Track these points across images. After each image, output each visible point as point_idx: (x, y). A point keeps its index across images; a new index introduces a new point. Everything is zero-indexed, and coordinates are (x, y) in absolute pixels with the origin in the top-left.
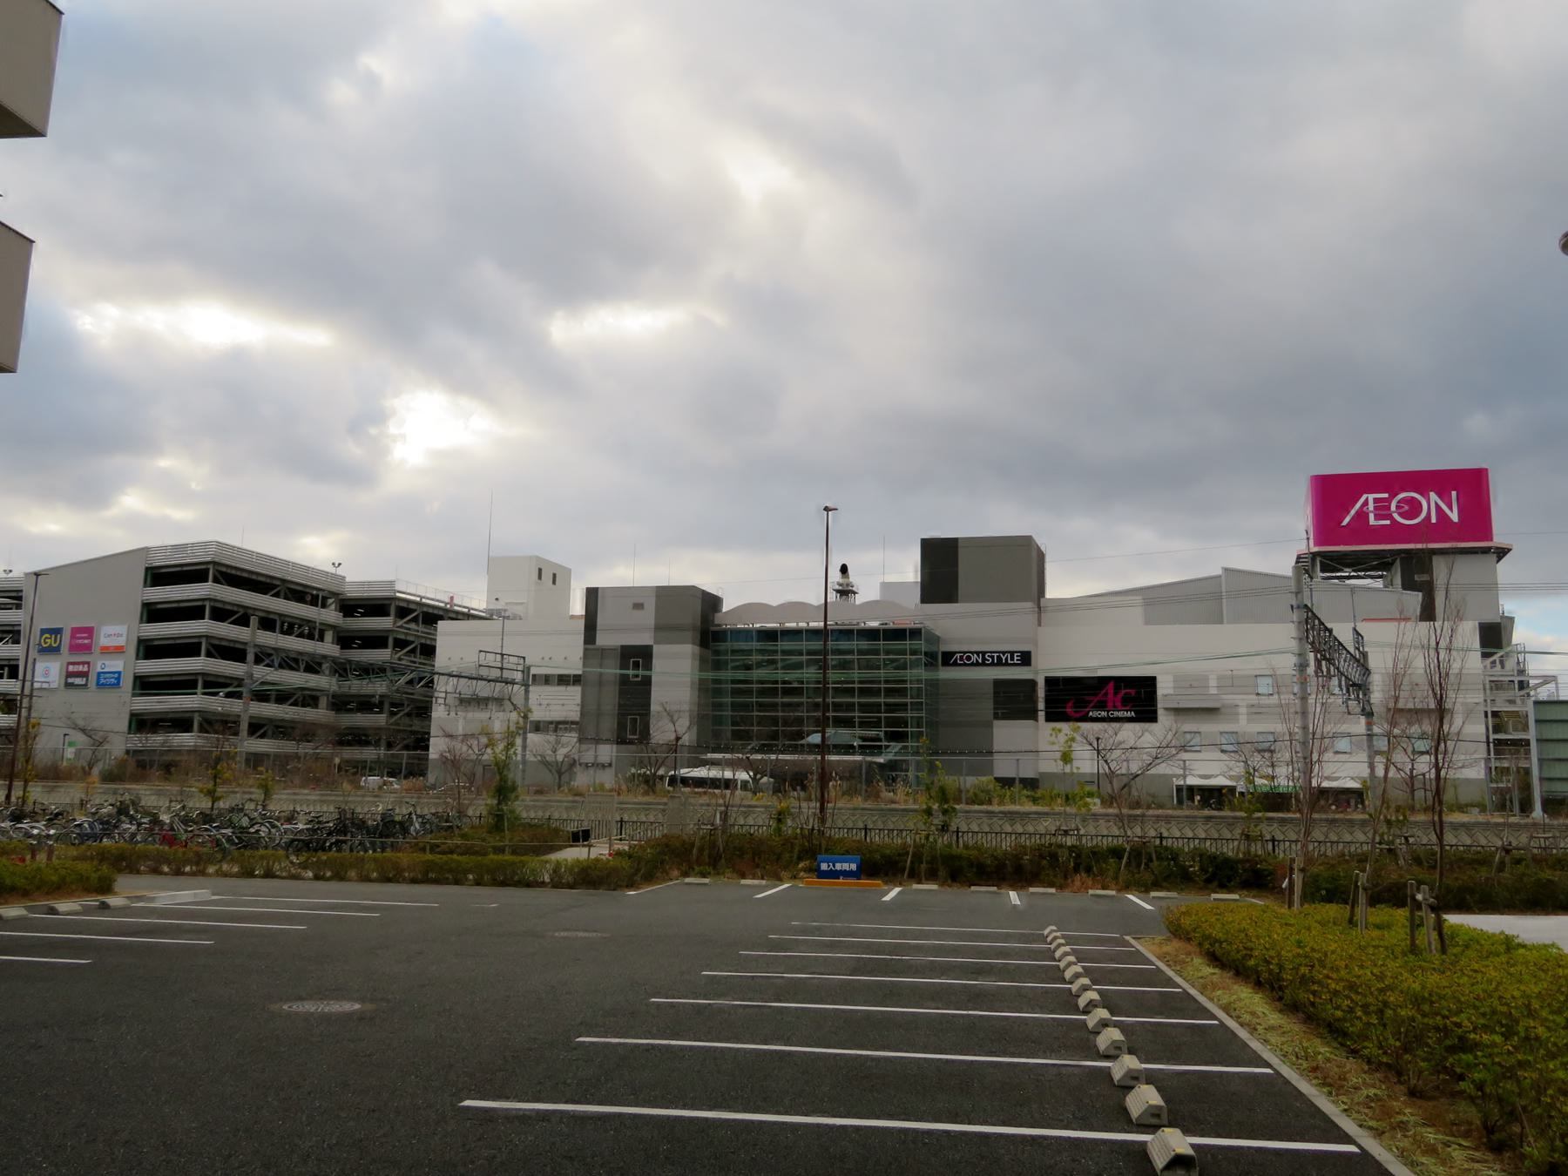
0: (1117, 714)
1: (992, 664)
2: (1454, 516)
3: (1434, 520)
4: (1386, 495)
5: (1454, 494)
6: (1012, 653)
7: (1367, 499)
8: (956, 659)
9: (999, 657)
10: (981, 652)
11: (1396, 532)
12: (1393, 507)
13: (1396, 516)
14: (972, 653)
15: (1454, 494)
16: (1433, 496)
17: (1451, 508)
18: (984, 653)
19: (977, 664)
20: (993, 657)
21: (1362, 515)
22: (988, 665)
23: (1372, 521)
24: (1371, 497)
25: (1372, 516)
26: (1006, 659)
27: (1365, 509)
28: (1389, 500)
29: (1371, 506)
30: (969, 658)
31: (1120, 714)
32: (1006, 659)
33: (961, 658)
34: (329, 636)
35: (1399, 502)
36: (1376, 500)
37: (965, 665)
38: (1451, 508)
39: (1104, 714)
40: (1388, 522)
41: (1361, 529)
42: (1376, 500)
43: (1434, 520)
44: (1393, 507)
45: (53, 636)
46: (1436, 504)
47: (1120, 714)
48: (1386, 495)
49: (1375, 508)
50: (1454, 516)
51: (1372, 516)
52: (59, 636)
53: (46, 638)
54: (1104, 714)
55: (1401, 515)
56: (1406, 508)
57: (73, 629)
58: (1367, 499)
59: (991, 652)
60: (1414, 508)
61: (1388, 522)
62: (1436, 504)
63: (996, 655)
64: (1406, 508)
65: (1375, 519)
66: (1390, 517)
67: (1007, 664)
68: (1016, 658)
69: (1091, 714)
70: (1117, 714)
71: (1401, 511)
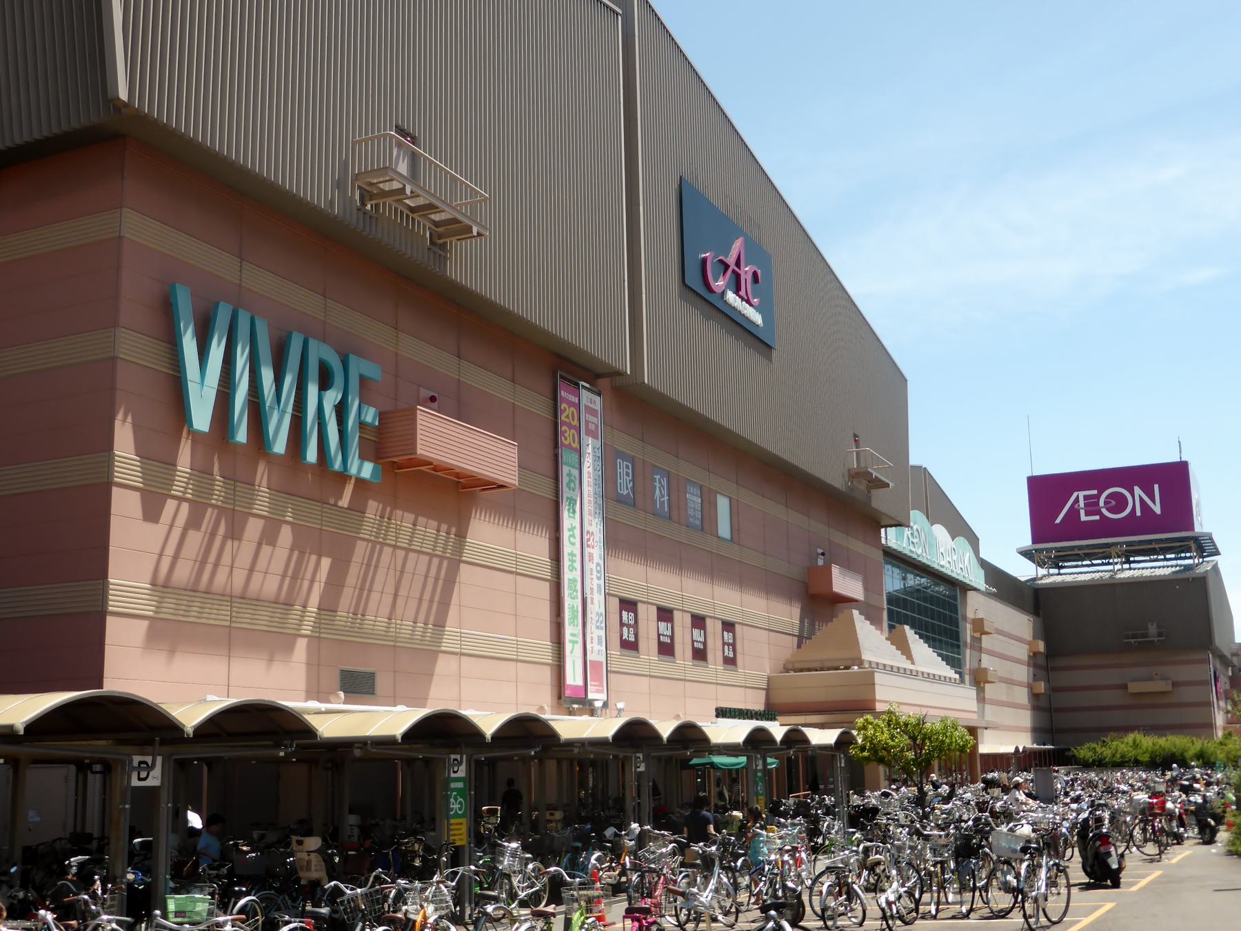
2: (1157, 509)
3: (1138, 513)
4: (1095, 492)
5: (1156, 487)
7: (1078, 496)
11: (1106, 528)
13: (1104, 511)
15: (1156, 487)
16: (1138, 491)
17: (1154, 501)
21: (1074, 512)
23: (1083, 518)
24: (1082, 494)
25: (1082, 512)
27: (1076, 506)
28: (1098, 497)
29: (1082, 503)
35: (1106, 498)
36: (1086, 498)
38: (1154, 502)
40: (1097, 518)
41: (1073, 528)
42: (1086, 498)
43: (1138, 513)
44: (1102, 503)
46: (1141, 499)
48: (1095, 492)
49: (1086, 505)
50: (1157, 509)
51: (1082, 512)
55: (1111, 510)
56: (1113, 503)
58: (1078, 496)
60: (1118, 503)
61: (1097, 518)
62: (1141, 499)
64: (1113, 503)
65: (1087, 514)
71: (1109, 505)
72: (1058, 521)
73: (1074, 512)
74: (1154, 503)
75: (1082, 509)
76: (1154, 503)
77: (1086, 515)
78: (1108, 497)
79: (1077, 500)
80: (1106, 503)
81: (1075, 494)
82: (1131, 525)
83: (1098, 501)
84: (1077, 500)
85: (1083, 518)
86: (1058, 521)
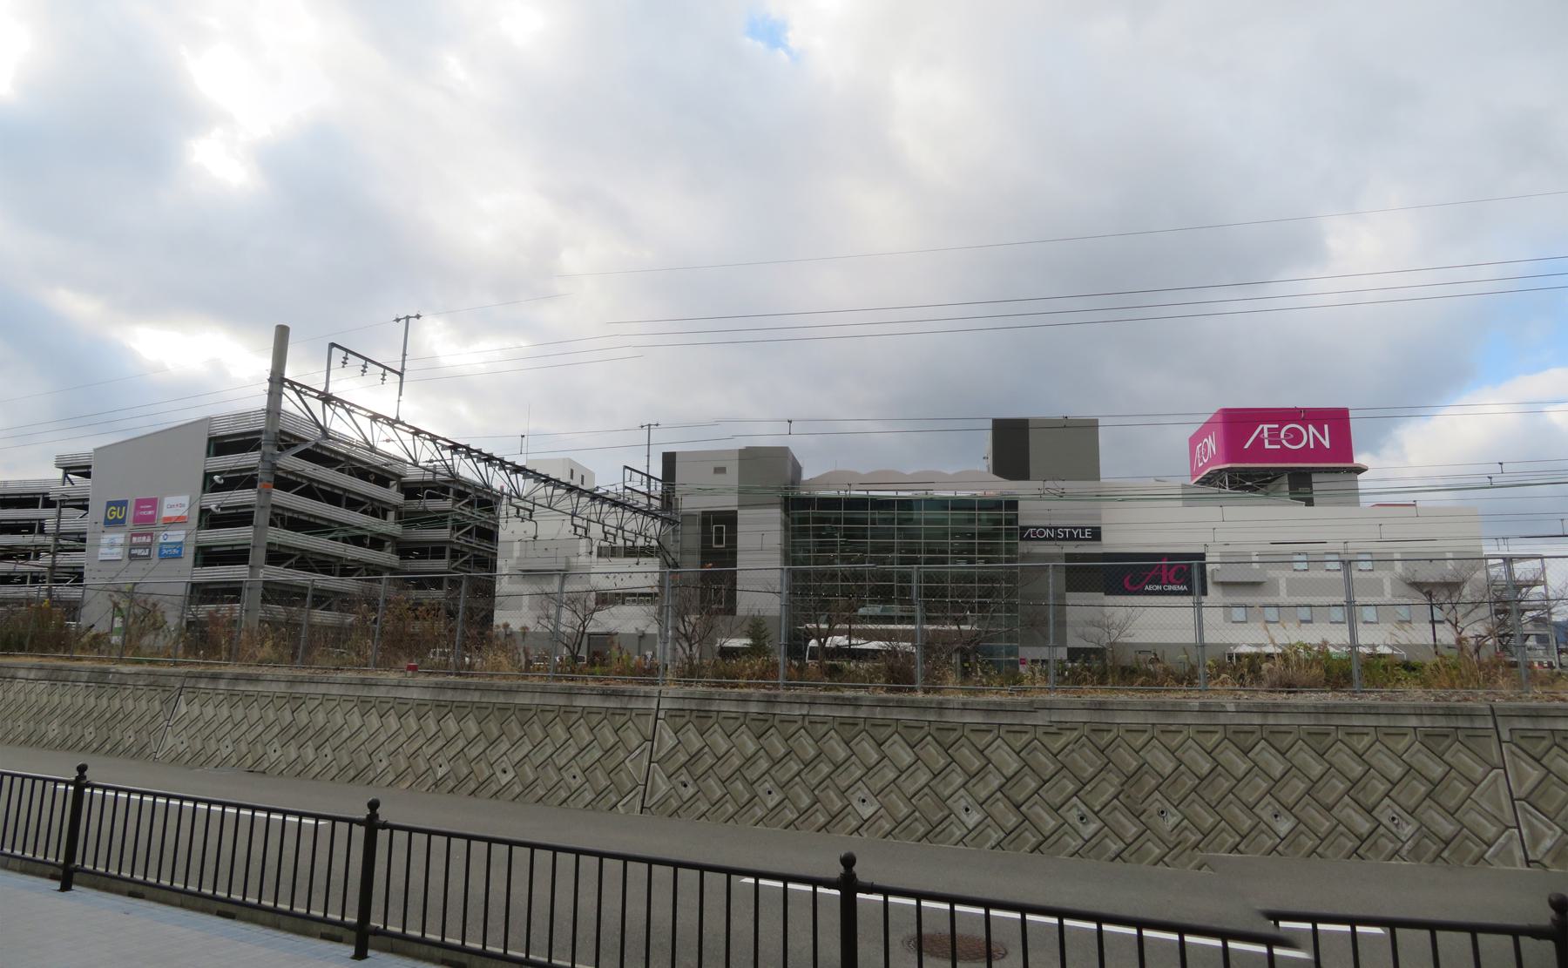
0: (1170, 588)
1: (1065, 539)
2: (1327, 444)
3: (1312, 446)
4: (1277, 426)
5: (1326, 427)
6: (1083, 528)
8: (1029, 534)
9: (1071, 533)
10: (1053, 528)
11: (1284, 454)
12: (1282, 436)
13: (1284, 442)
14: (1045, 528)
15: (1326, 427)
16: (1310, 427)
17: (1324, 437)
18: (1056, 528)
19: (1050, 539)
20: (1065, 533)
21: (1259, 441)
22: (1060, 540)
23: (1267, 446)
24: (1266, 427)
25: (1266, 442)
26: (1078, 534)
27: (1261, 436)
28: (1279, 430)
30: (1042, 533)
31: (1174, 588)
32: (1078, 534)
33: (1034, 533)
34: (391, 515)
36: (1269, 430)
37: (1038, 539)
38: (1324, 437)
39: (1158, 588)
40: (1279, 447)
41: (1258, 451)
42: (1269, 430)
43: (1312, 446)
44: (1282, 436)
45: (119, 509)
47: (1174, 588)
48: (1277, 426)
50: (1327, 444)
51: (1266, 442)
52: (124, 508)
53: (113, 510)
54: (1158, 588)
56: (1292, 436)
57: (137, 500)
59: (1063, 528)
60: (1296, 437)
61: (1279, 447)
63: (1067, 530)
64: (1292, 436)
66: (1280, 443)
67: (1078, 539)
68: (1086, 533)
69: (1147, 588)
70: (1170, 588)
72: (1246, 447)
73: (1259, 441)
78: (1288, 431)
79: (1262, 431)
81: (1261, 426)
82: (1305, 454)
84: (1262, 431)
85: (1267, 446)
86: (1246, 447)
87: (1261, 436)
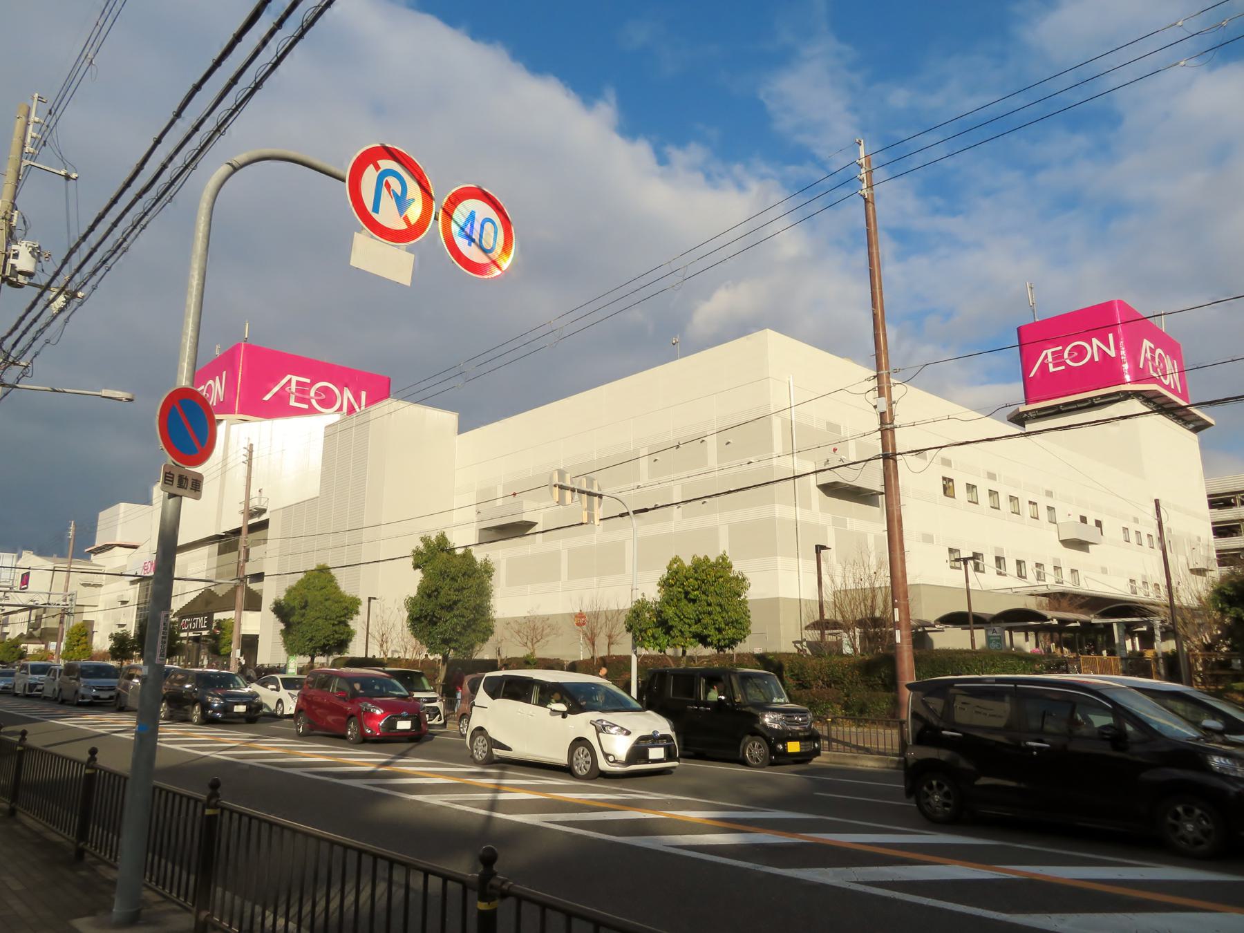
3: (1096, 359)
4: (1060, 348)
13: (1068, 362)
16: (1095, 341)
17: (1109, 347)
21: (1044, 366)
23: (1052, 369)
24: (1049, 352)
25: (1051, 366)
28: (1063, 351)
29: (1050, 358)
35: (1070, 351)
36: (1053, 353)
38: (1109, 347)
40: (1063, 368)
42: (1053, 353)
43: (1096, 359)
44: (1066, 355)
46: (1098, 347)
48: (1060, 348)
49: (1054, 359)
55: (1073, 360)
56: (1076, 354)
60: (1081, 352)
61: (1063, 368)
62: (1099, 348)
64: (1076, 354)
65: (1055, 365)
66: (1064, 363)
73: (1044, 366)
74: (1110, 349)
75: (1051, 362)
76: (1110, 349)
77: (1055, 365)
79: (1046, 357)
80: (1070, 355)
83: (1063, 355)
84: (1046, 357)
85: (1052, 369)
87: (1046, 361)
